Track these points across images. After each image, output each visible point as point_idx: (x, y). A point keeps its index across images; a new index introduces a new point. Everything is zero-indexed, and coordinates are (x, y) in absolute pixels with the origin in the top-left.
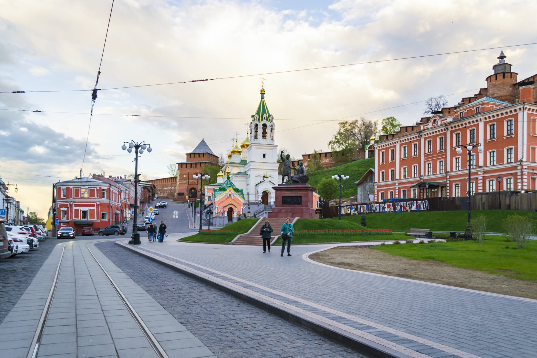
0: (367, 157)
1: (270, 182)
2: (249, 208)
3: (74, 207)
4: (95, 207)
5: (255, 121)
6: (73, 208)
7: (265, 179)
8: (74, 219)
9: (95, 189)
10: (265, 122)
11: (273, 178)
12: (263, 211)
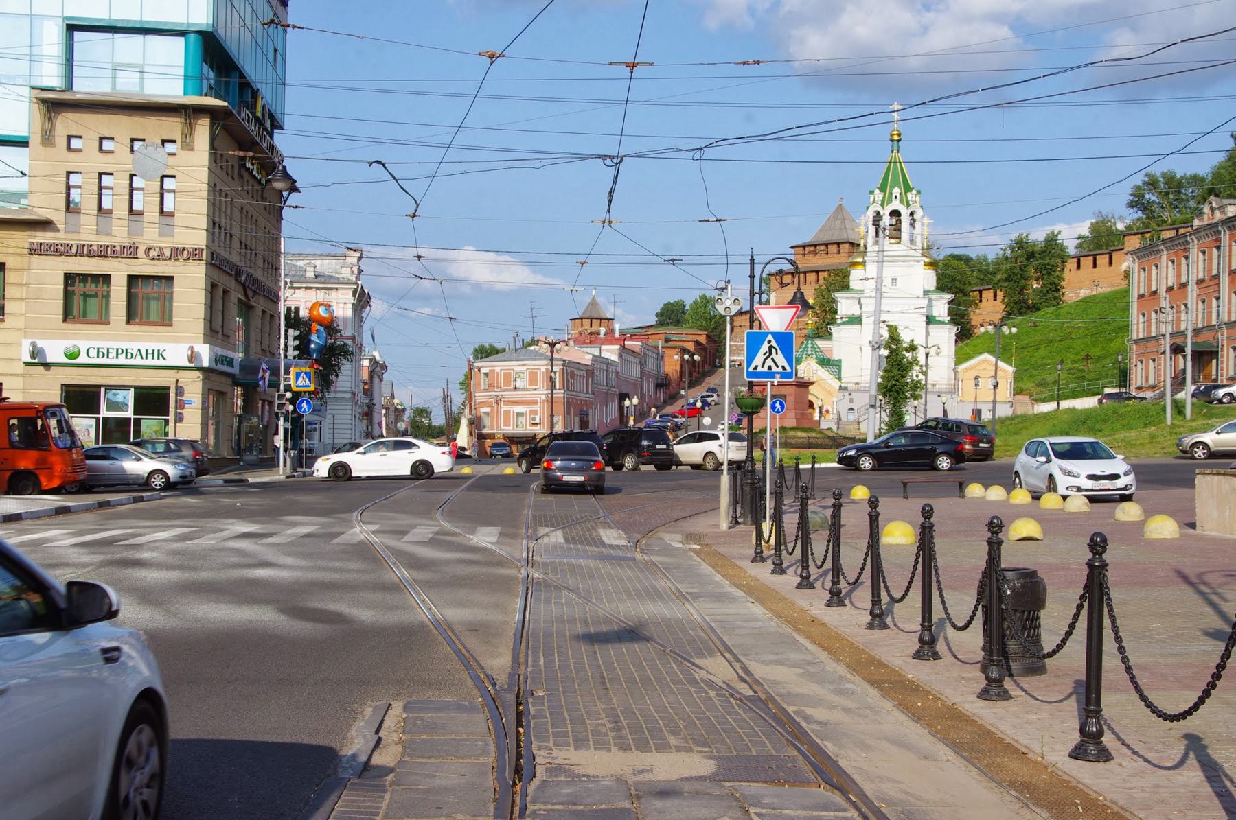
8: (502, 427)
10: (896, 205)
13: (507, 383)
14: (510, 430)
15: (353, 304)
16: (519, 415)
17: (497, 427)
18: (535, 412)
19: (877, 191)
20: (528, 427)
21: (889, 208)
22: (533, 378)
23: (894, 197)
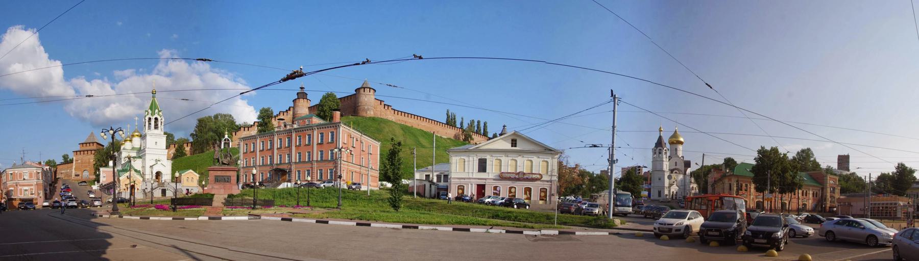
2: (146, 185)
7: (158, 162)
10: (156, 116)
13: (20, 177)
14: (22, 197)
16: (26, 190)
19: (149, 111)
21: (154, 117)
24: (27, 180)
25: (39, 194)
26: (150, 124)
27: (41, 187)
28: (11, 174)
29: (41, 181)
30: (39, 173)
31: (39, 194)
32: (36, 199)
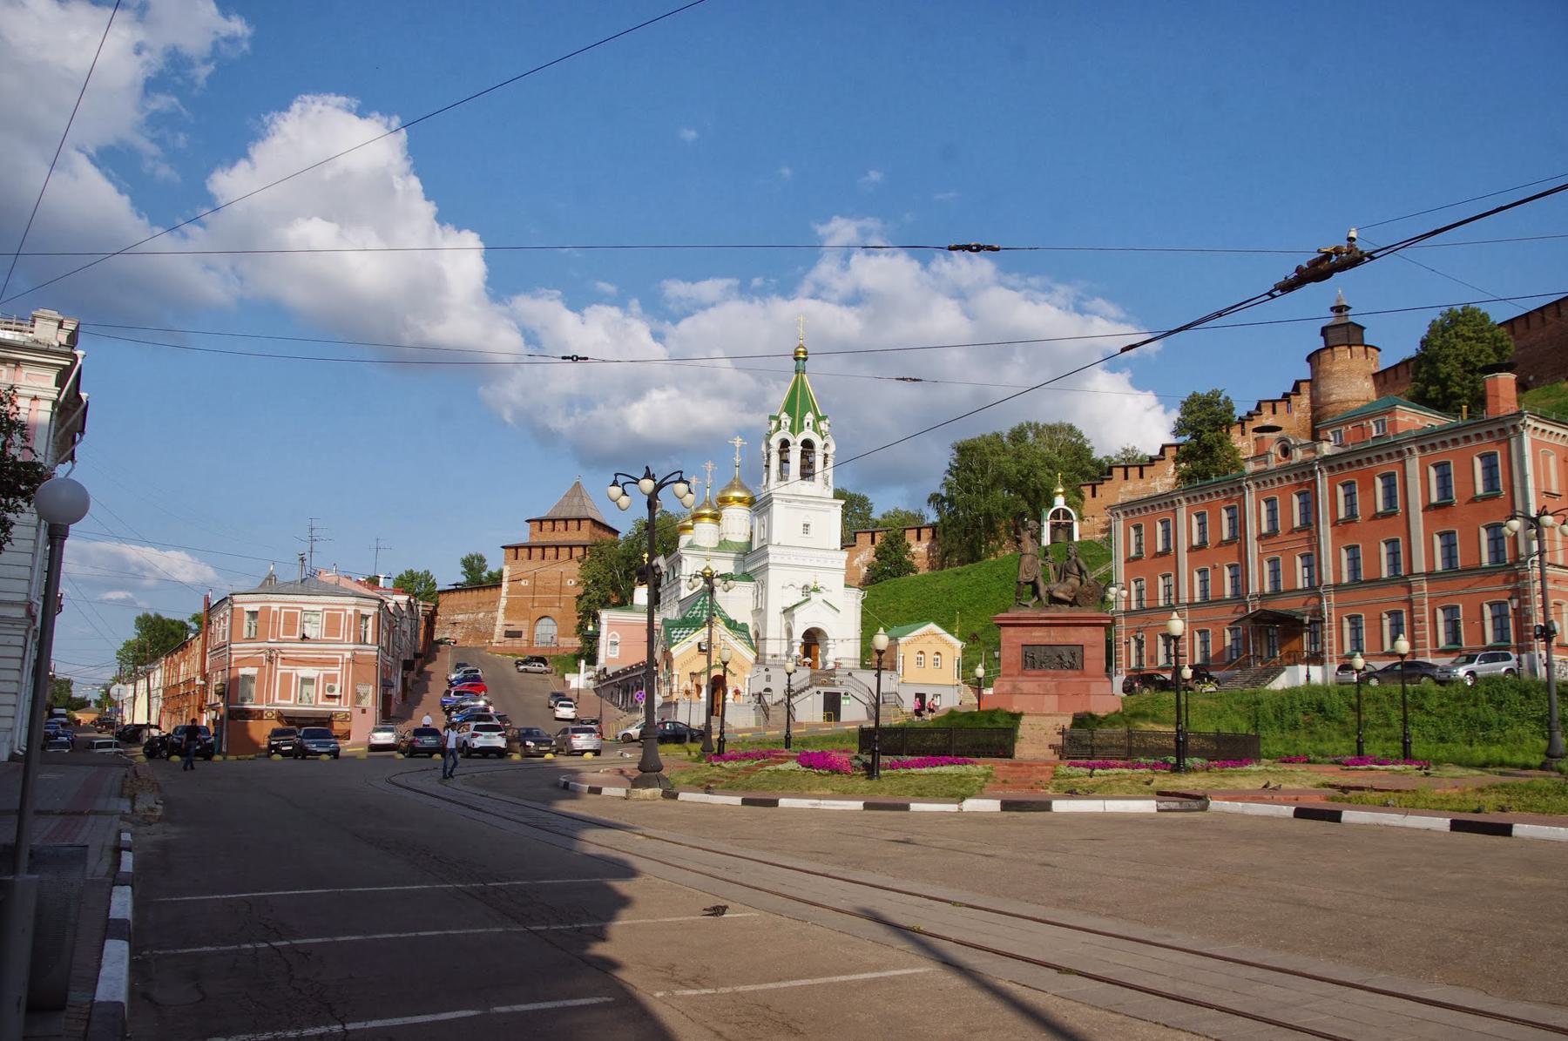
0: (1046, 540)
1: (824, 605)
3: (279, 666)
4: (340, 668)
5: (782, 431)
6: (276, 669)
8: (277, 701)
9: (343, 613)
10: (807, 433)
11: (831, 591)
12: (810, 686)
14: (290, 705)
15: (55, 403)
16: (308, 681)
17: (268, 700)
18: (333, 678)
19: (784, 416)
20: (320, 703)
21: (801, 437)
22: (332, 624)
23: (806, 424)
24: (316, 641)
25: (358, 698)
26: (784, 461)
27: (372, 673)
28: (253, 614)
29: (371, 650)
30: (366, 617)
31: (358, 698)
32: (347, 717)
